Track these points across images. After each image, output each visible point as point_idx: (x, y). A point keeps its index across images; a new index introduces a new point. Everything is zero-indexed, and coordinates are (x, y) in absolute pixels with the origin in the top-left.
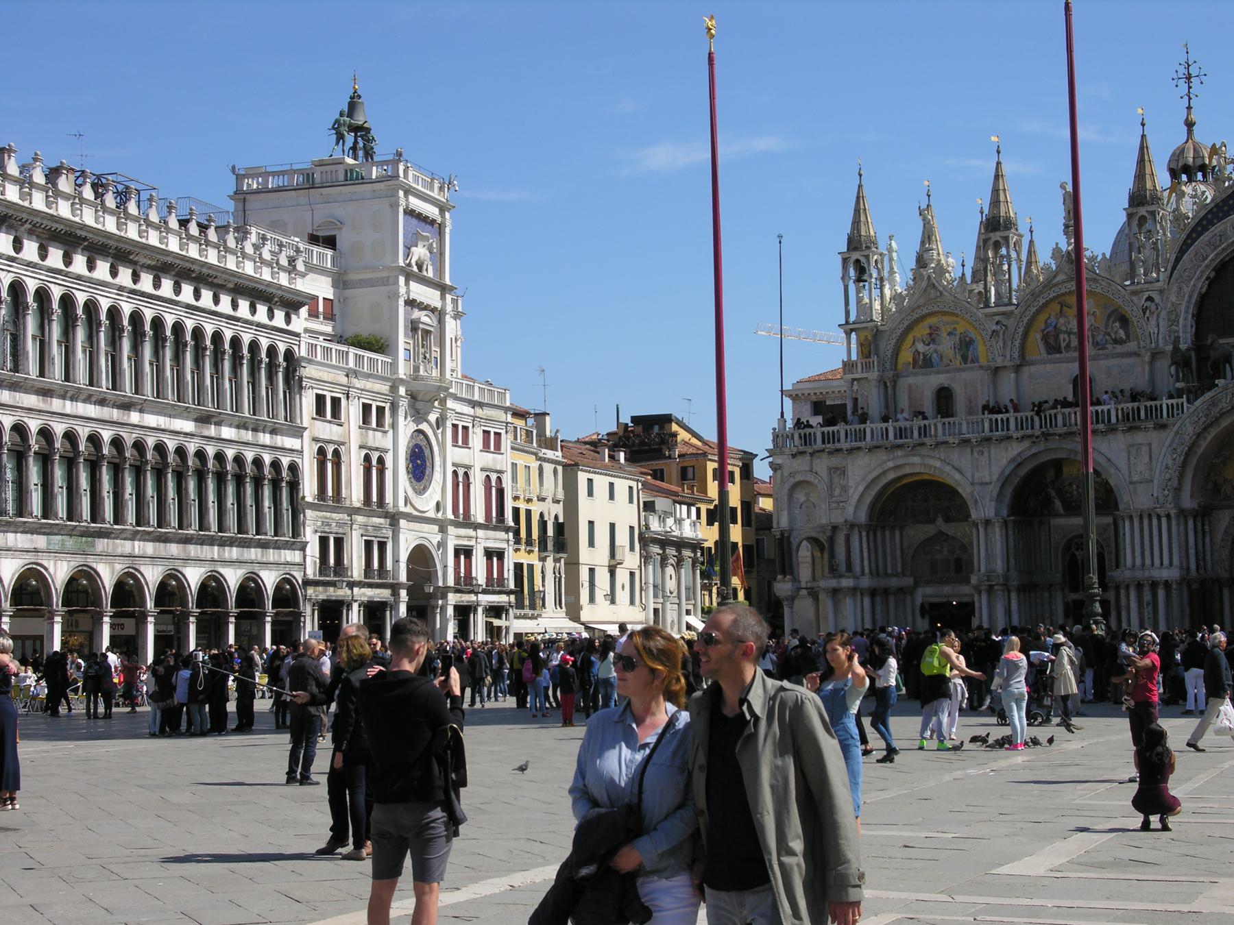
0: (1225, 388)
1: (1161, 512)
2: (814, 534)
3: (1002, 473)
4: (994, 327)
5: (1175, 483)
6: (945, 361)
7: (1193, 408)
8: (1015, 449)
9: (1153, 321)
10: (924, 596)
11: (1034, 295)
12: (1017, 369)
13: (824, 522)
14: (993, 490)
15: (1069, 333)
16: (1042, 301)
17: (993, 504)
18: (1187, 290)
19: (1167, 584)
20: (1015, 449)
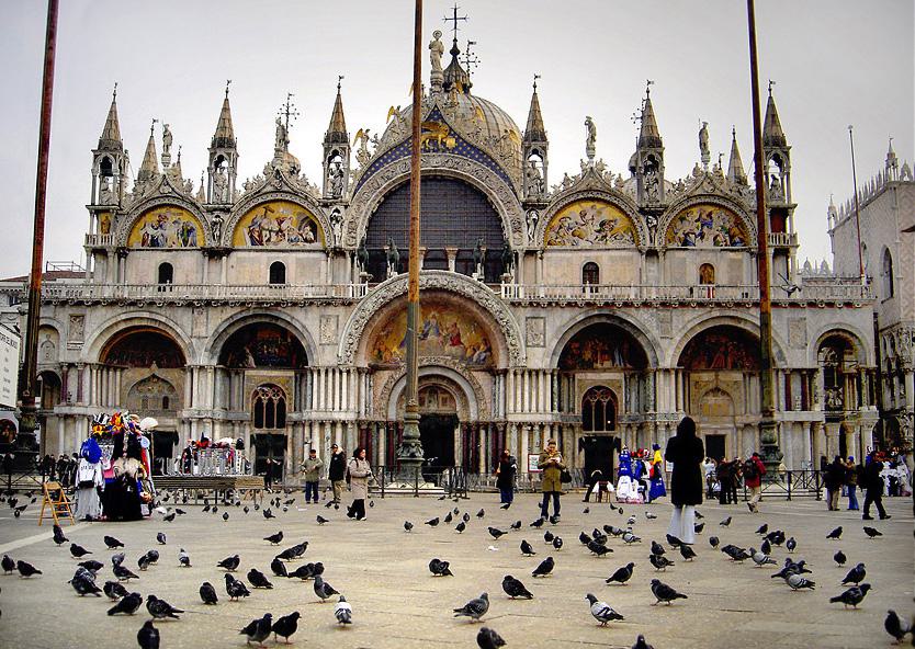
5: (355, 347)
6: (170, 243)
8: (229, 312)
9: (338, 226)
11: (247, 199)
12: (228, 252)
13: (61, 360)
14: (208, 342)
18: (364, 208)
19: (344, 424)
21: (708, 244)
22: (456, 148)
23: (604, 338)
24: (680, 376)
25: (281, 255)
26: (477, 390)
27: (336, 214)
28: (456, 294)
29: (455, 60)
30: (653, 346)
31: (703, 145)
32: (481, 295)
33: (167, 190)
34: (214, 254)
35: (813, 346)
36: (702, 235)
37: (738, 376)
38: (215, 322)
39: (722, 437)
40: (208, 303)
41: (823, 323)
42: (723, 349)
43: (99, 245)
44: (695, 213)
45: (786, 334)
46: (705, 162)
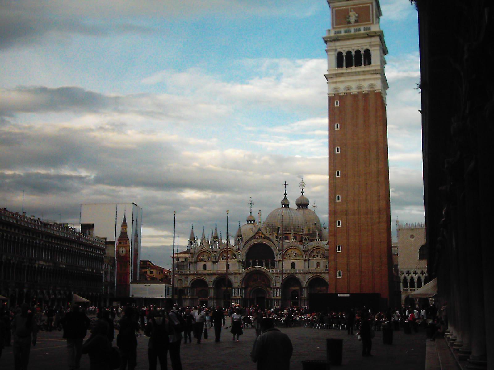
1: (239, 288)
4: (214, 255)
8: (216, 276)
9: (239, 256)
11: (221, 250)
12: (217, 262)
14: (212, 283)
18: (245, 251)
20: (216, 276)
21: (319, 257)
23: (291, 281)
26: (268, 292)
27: (239, 253)
29: (285, 196)
30: (302, 282)
33: (204, 248)
34: (214, 262)
36: (317, 256)
37: (325, 288)
38: (214, 278)
40: (212, 274)
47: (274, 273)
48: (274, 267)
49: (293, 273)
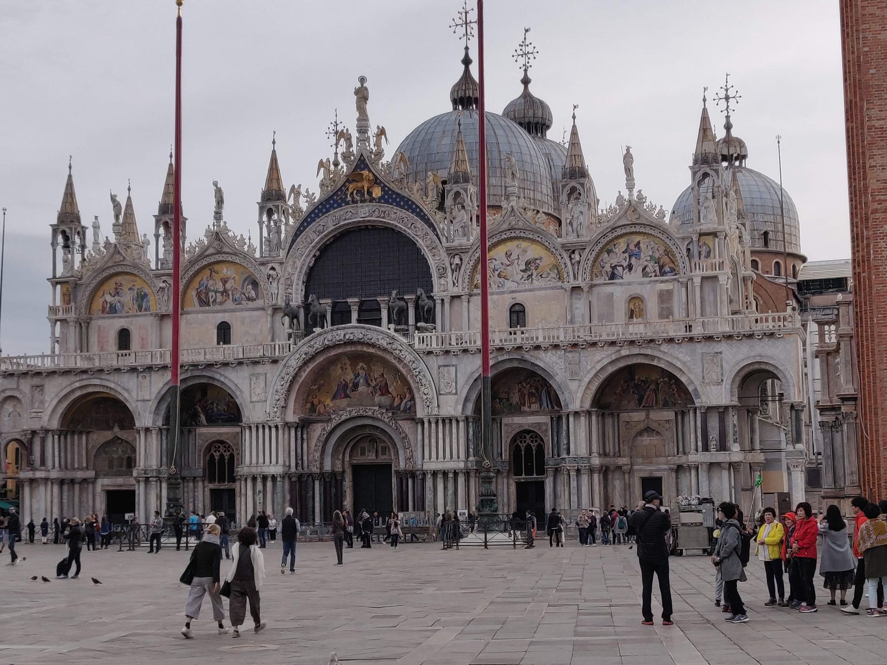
0: (320, 335)
1: (272, 424)
2: (18, 437)
3: (159, 393)
4: (162, 285)
5: (283, 404)
7: (296, 347)
9: (275, 284)
10: (103, 486)
11: (192, 263)
13: (25, 428)
14: (152, 405)
15: (216, 292)
16: (197, 267)
17: (152, 416)
18: (299, 264)
19: (274, 478)
22: (382, 197)
23: (513, 384)
24: (594, 418)
25: (227, 314)
27: (271, 272)
28: (373, 345)
29: (467, 70)
31: (628, 171)
32: (394, 346)
33: (118, 258)
35: (730, 381)
36: (630, 267)
37: (669, 415)
38: (159, 383)
39: (659, 479)
40: (150, 368)
41: (741, 356)
42: (652, 387)
43: (60, 316)
44: (622, 244)
45: (700, 370)
46: (630, 186)
47: (430, 353)
48: (429, 325)
49: (520, 348)
